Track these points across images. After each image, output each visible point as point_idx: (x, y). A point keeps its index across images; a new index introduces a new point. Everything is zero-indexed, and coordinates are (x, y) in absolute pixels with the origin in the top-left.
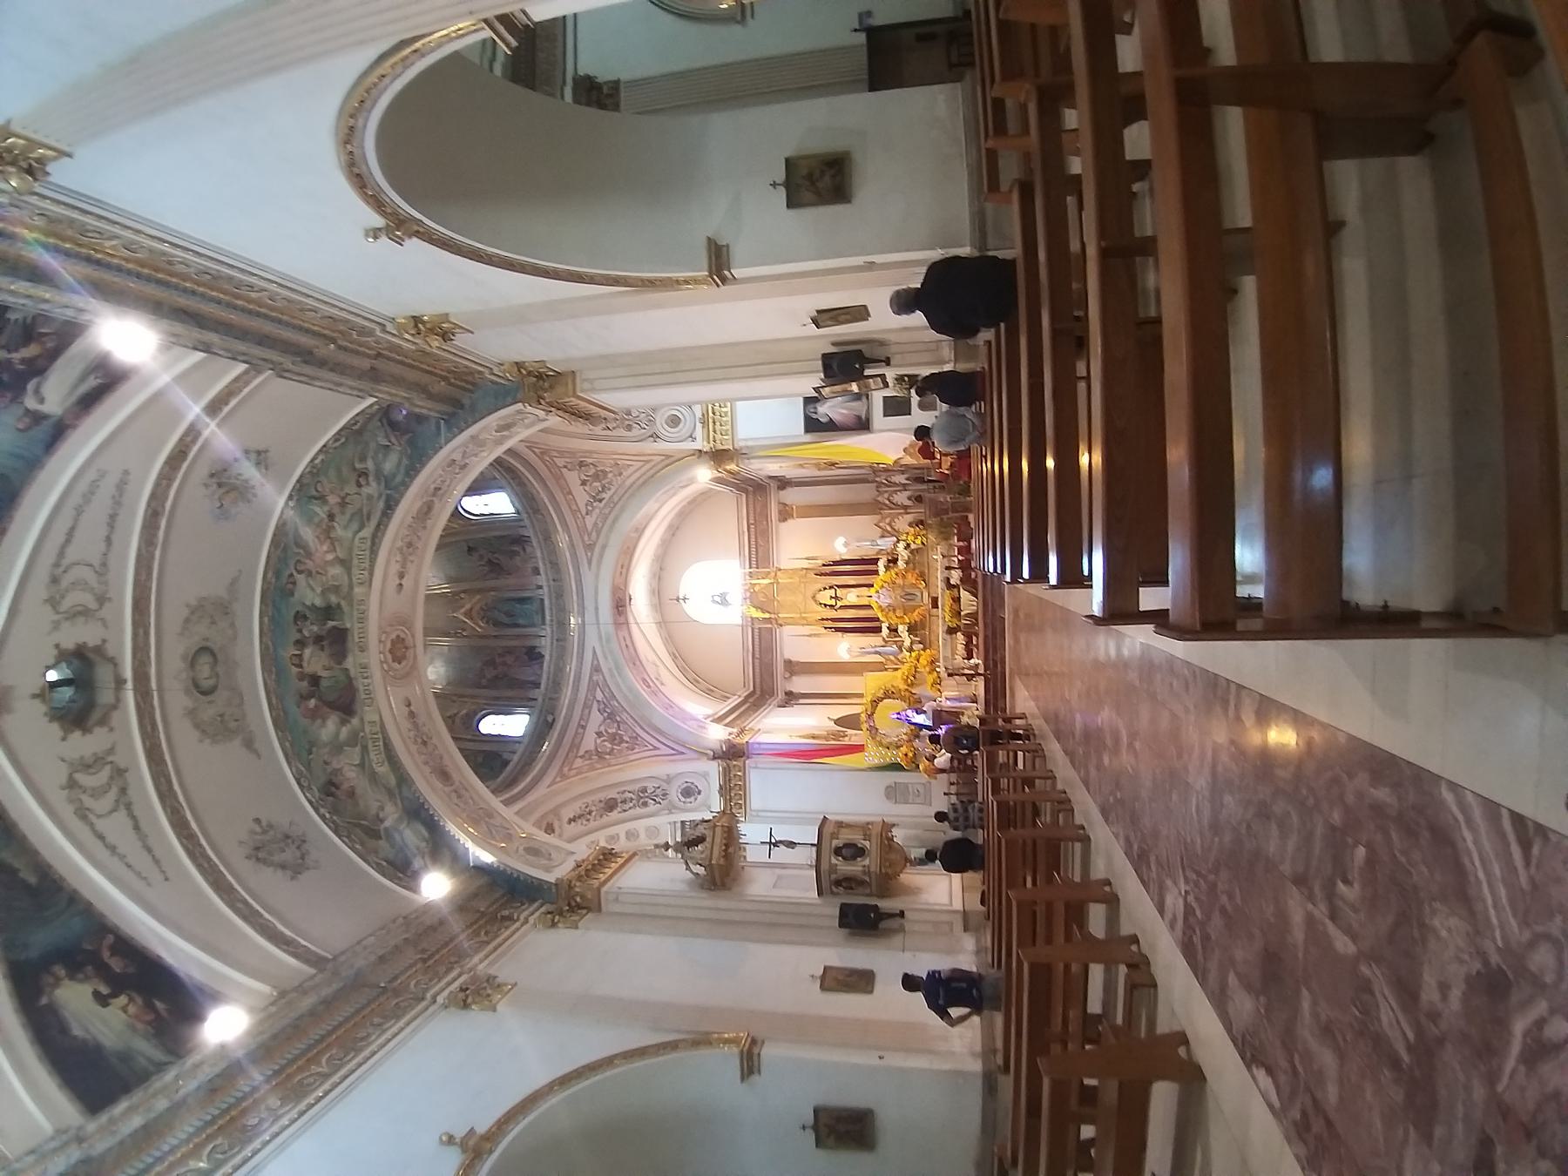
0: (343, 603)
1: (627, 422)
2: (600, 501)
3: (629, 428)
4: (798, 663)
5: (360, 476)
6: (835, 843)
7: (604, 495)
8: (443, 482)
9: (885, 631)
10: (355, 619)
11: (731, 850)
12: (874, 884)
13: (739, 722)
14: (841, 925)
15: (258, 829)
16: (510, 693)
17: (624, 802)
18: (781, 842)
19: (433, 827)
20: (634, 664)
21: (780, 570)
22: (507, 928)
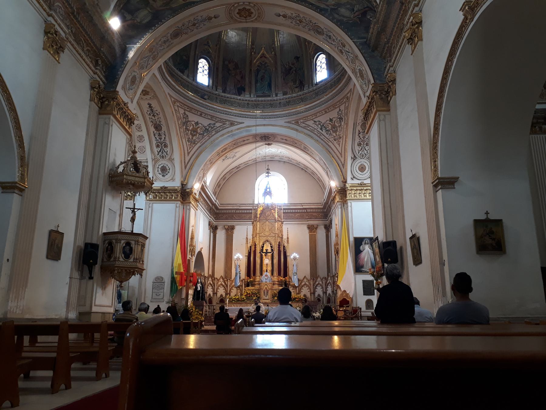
1: (362, 143)
2: (321, 129)
3: (359, 145)
4: (233, 233)
6: (133, 242)
7: (324, 131)
8: (334, 41)
11: (131, 186)
13: (202, 200)
14: (86, 245)
16: (220, 76)
17: (160, 135)
18: (135, 214)
20: (235, 144)
21: (282, 223)
22: (91, 62)
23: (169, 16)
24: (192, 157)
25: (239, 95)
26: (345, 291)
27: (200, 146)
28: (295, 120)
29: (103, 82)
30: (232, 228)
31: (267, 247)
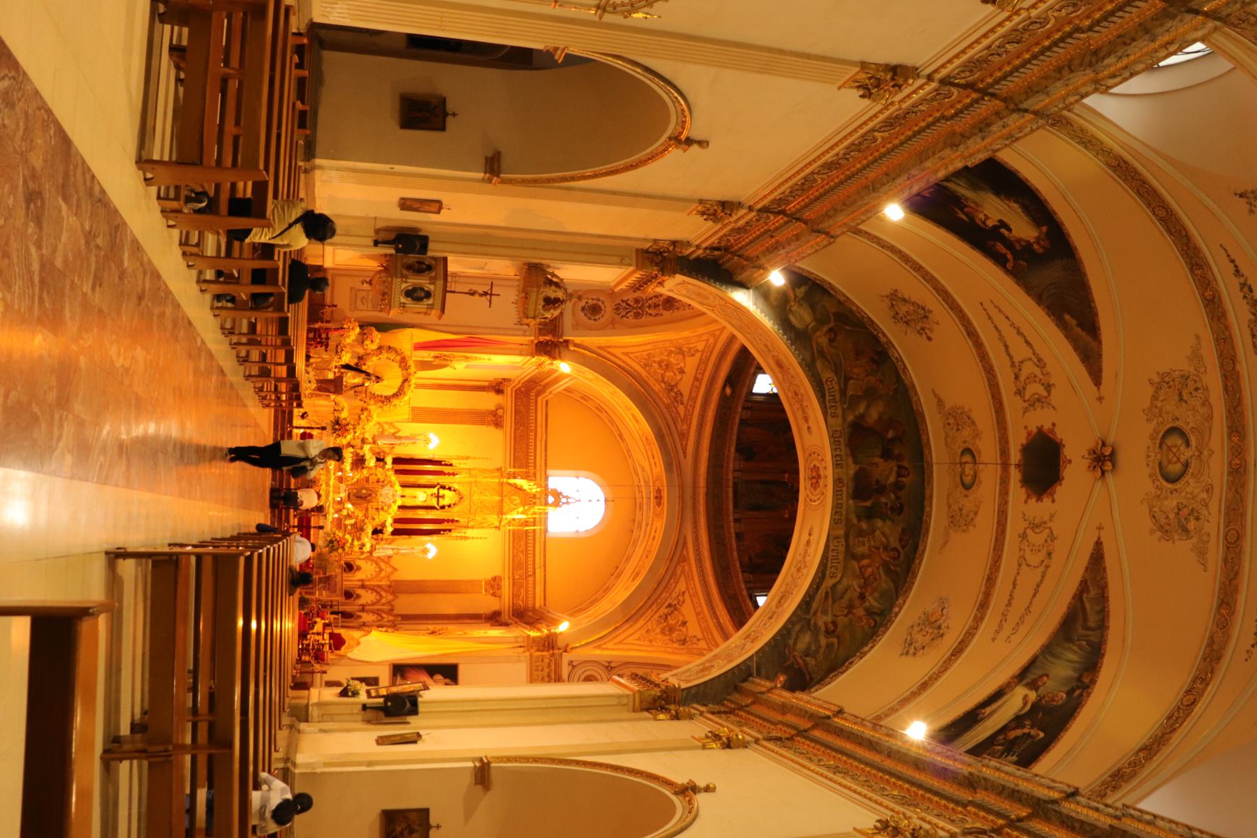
0: (855, 521)
2: (670, 605)
4: (489, 424)
5: (834, 631)
6: (430, 301)
7: (666, 611)
8: (765, 624)
9: (389, 460)
10: (844, 507)
12: (399, 265)
15: (926, 331)
17: (656, 306)
18: (481, 295)
19: (785, 323)
20: (647, 439)
21: (496, 527)
23: (801, 357)
24: (620, 359)
25: (737, 450)
26: (358, 643)
27: (641, 376)
28: (688, 556)
29: (688, 255)
30: (498, 423)
31: (449, 497)
